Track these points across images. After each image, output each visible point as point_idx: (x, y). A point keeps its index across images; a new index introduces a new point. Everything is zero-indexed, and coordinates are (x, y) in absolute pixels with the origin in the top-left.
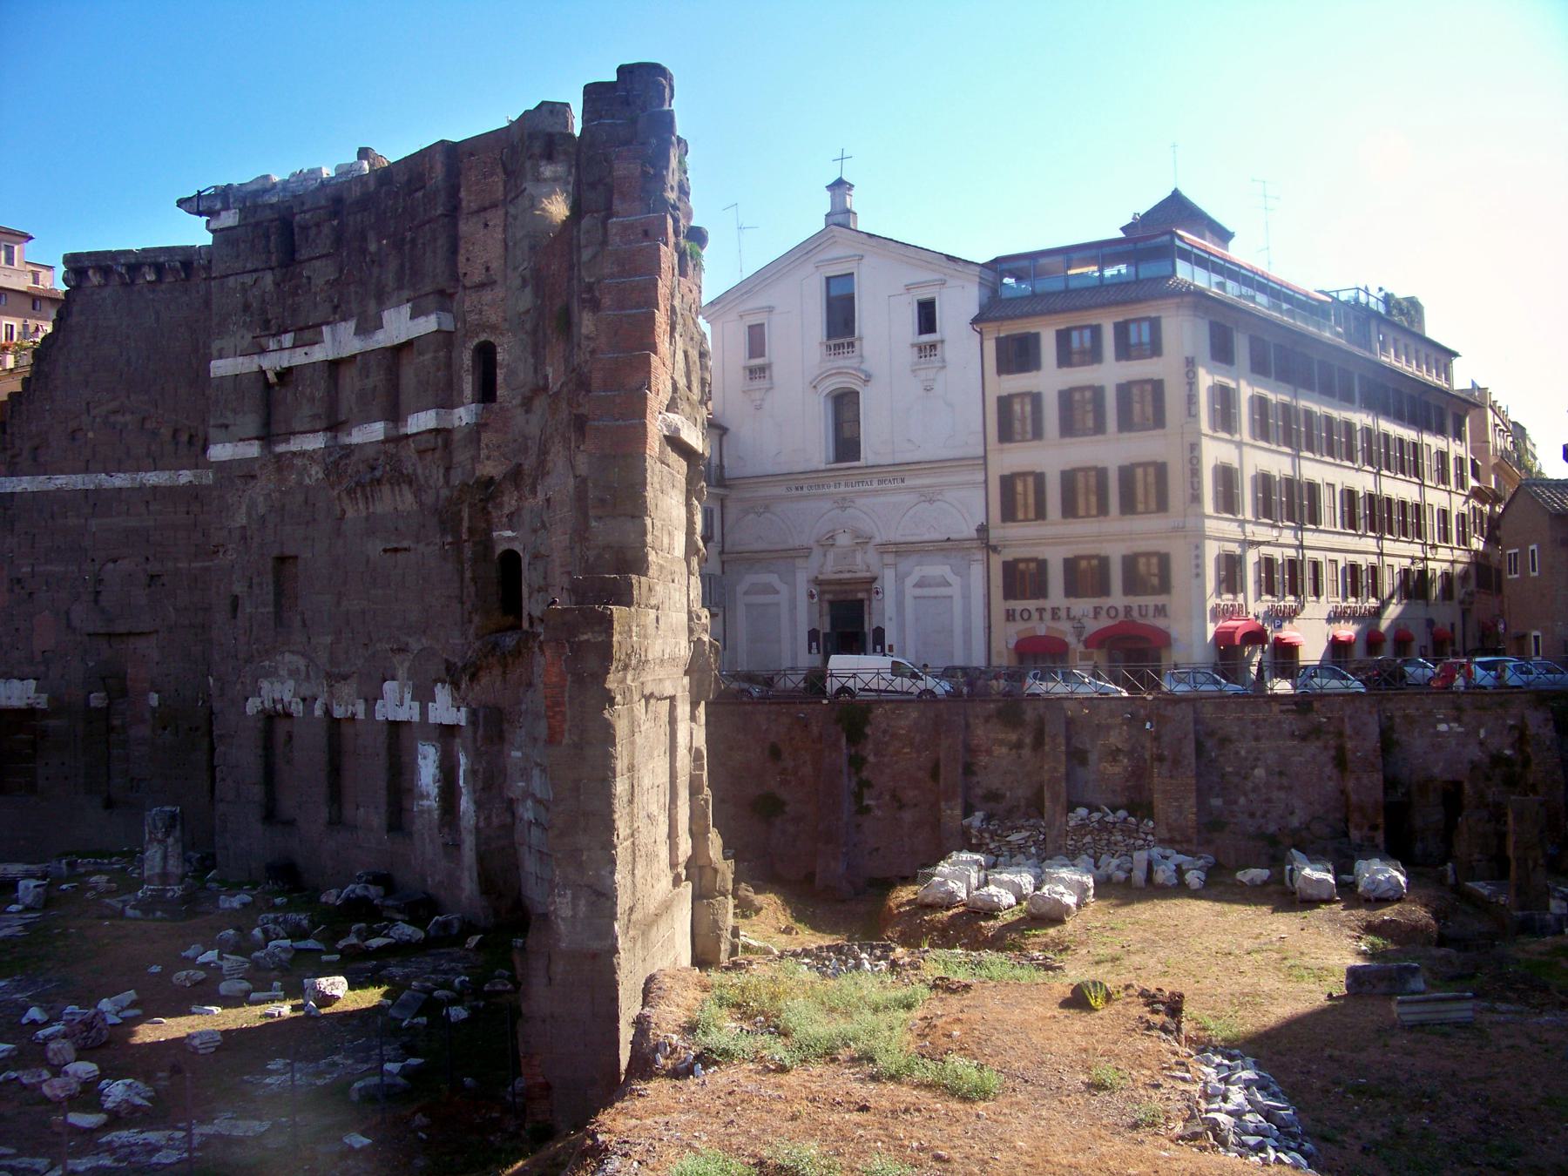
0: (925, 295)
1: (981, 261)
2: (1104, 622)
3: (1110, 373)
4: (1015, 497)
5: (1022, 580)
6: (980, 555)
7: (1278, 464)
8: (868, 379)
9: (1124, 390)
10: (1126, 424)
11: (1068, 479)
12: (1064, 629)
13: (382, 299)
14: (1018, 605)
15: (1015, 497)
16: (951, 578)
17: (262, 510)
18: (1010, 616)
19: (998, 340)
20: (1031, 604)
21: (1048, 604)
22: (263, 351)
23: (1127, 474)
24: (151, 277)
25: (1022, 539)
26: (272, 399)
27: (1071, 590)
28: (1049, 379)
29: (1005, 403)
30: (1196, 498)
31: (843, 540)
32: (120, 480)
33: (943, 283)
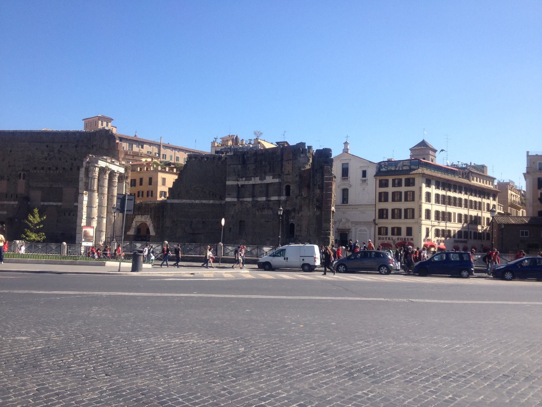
0: (364, 169)
1: (376, 162)
2: (400, 241)
3: (403, 189)
4: (382, 214)
5: (382, 231)
6: (373, 225)
7: (441, 208)
8: (351, 186)
9: (406, 193)
10: (406, 200)
11: (393, 210)
12: (391, 242)
13: (266, 174)
14: (381, 236)
15: (382, 214)
16: (367, 229)
17: (237, 211)
18: (379, 239)
19: (380, 180)
20: (384, 237)
21: (388, 236)
22: (238, 181)
23: (406, 210)
24: (206, 160)
25: (383, 223)
26: (240, 191)
27: (393, 234)
28: (390, 189)
29: (380, 194)
30: (420, 216)
31: (344, 220)
32: (197, 202)
33: (368, 167)
